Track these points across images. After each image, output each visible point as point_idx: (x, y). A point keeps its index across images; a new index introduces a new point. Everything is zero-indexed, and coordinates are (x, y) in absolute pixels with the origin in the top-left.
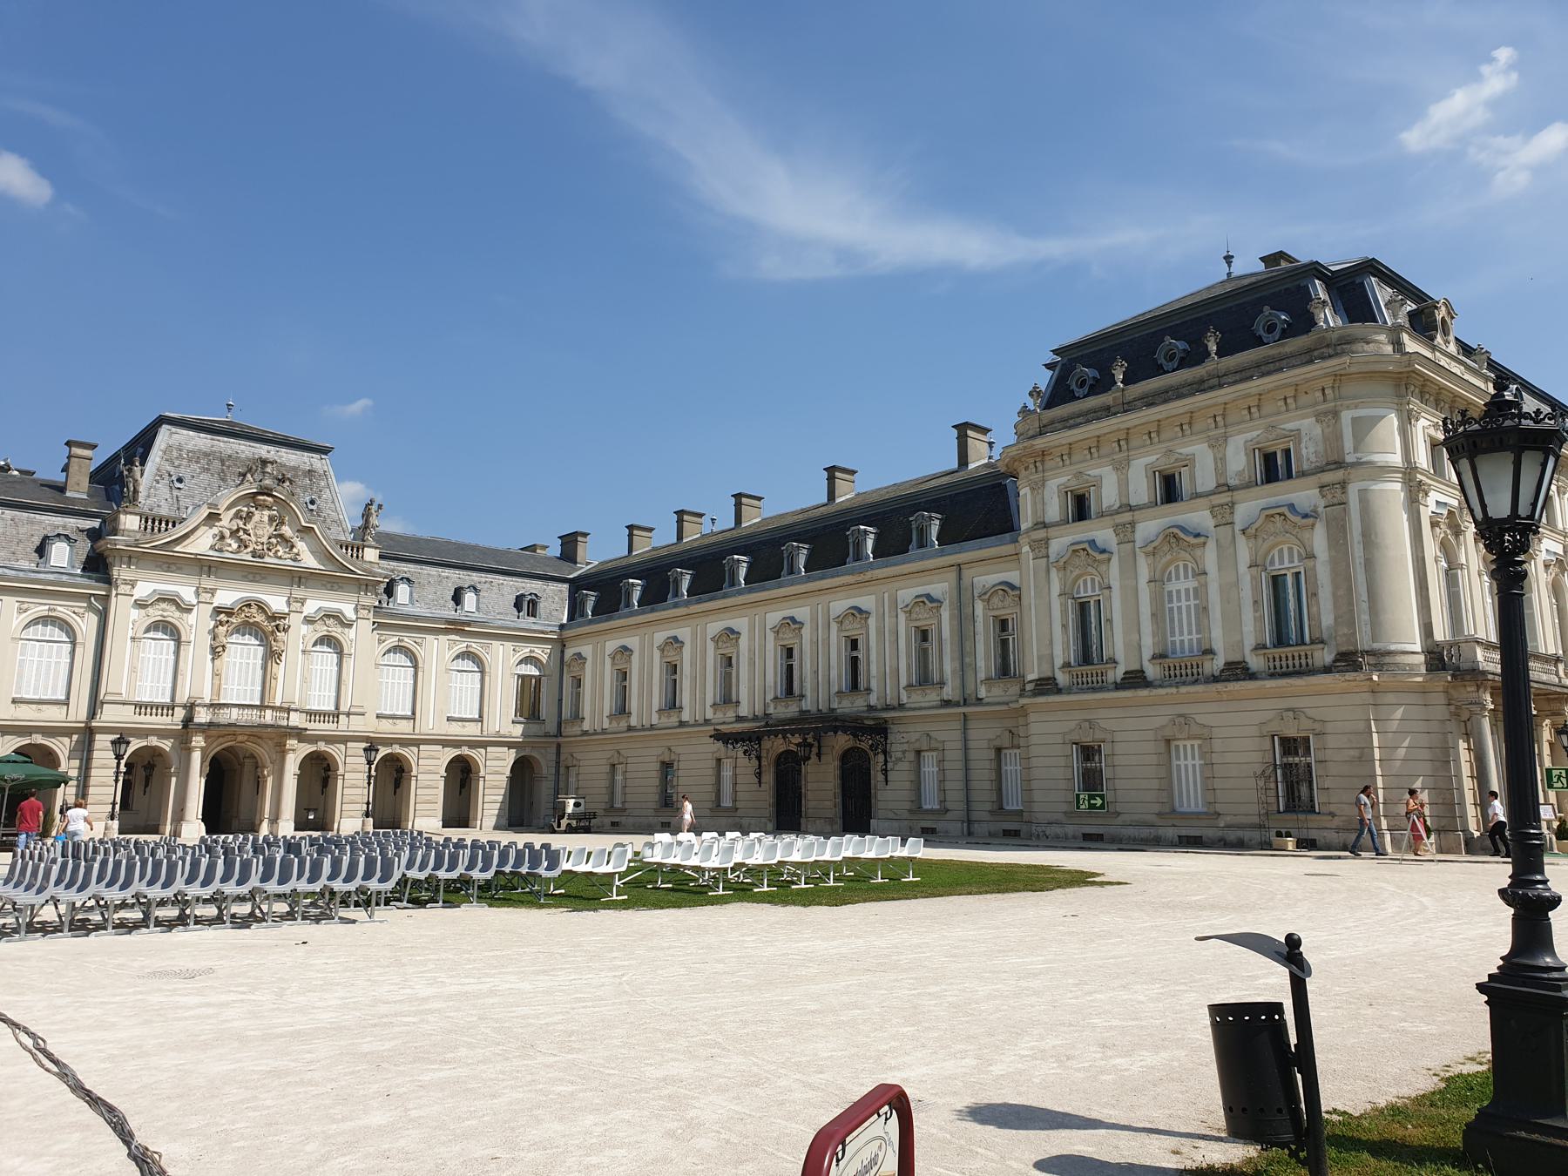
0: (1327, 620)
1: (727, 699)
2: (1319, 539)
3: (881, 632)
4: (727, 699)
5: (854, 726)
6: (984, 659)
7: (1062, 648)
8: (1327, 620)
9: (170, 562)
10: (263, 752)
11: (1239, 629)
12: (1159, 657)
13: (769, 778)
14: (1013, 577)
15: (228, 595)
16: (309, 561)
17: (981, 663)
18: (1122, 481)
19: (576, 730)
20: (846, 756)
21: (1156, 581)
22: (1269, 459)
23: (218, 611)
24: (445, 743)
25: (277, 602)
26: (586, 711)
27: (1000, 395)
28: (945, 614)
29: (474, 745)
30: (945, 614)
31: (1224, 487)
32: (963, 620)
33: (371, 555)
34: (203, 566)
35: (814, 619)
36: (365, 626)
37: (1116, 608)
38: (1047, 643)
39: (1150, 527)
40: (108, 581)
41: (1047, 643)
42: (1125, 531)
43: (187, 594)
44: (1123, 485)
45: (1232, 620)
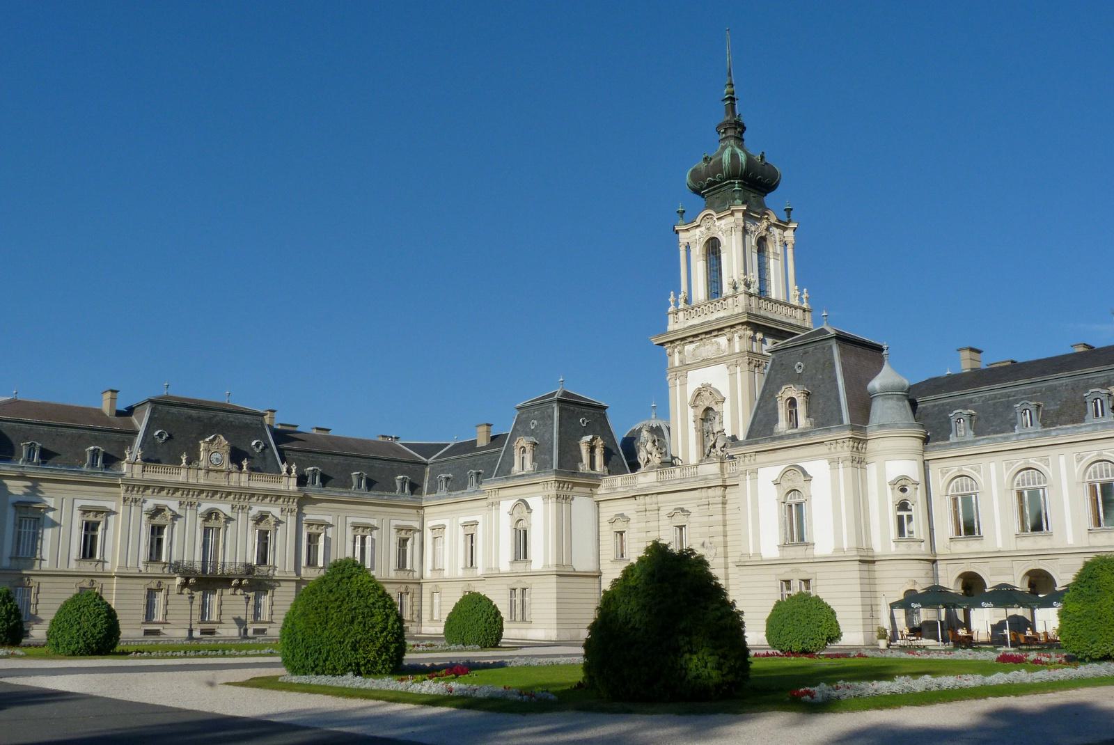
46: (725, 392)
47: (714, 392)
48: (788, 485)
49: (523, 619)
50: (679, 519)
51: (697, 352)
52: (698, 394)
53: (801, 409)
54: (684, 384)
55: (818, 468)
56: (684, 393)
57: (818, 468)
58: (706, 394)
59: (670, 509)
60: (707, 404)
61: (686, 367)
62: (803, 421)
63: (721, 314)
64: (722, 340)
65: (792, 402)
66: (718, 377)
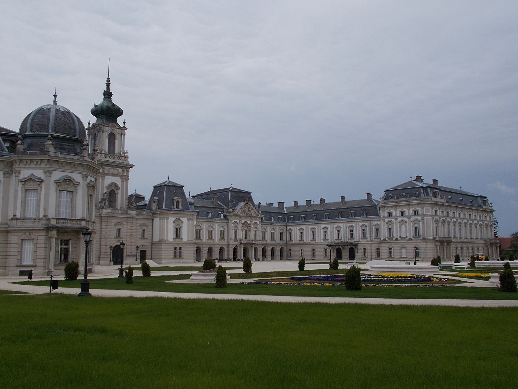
0: (421, 234)
1: (326, 239)
2: (421, 224)
3: (356, 229)
4: (326, 239)
5: (351, 244)
6: (374, 235)
7: (387, 235)
8: (421, 234)
9: (236, 216)
10: (249, 247)
11: (411, 234)
12: (400, 237)
13: (335, 252)
14: (379, 223)
15: (243, 222)
16: (253, 214)
17: (374, 236)
18: (396, 212)
19: (291, 243)
20: (350, 249)
21: (400, 227)
22: (415, 212)
23: (242, 224)
24: (271, 245)
25: (249, 222)
26: (293, 239)
27: (378, 196)
28: (368, 228)
29: (275, 245)
30: (368, 228)
31: (409, 215)
32: (371, 229)
33: (260, 212)
34: (240, 216)
35: (344, 226)
36: (260, 225)
37: (394, 230)
38: (384, 234)
39: (399, 219)
40: (228, 220)
41: (384, 234)
42: (396, 219)
43: (238, 221)
44: (396, 213)
45: (410, 233)
46: (120, 186)
47: (116, 186)
48: (177, 223)
49: (180, 257)
50: (119, 226)
51: (110, 170)
52: (110, 185)
53: (180, 204)
54: (103, 179)
55: (185, 220)
56: (103, 183)
57: (185, 220)
58: (113, 185)
59: (116, 222)
60: (113, 188)
61: (104, 174)
62: (180, 207)
63: (120, 161)
64: (120, 170)
65: (178, 202)
66: (117, 180)
